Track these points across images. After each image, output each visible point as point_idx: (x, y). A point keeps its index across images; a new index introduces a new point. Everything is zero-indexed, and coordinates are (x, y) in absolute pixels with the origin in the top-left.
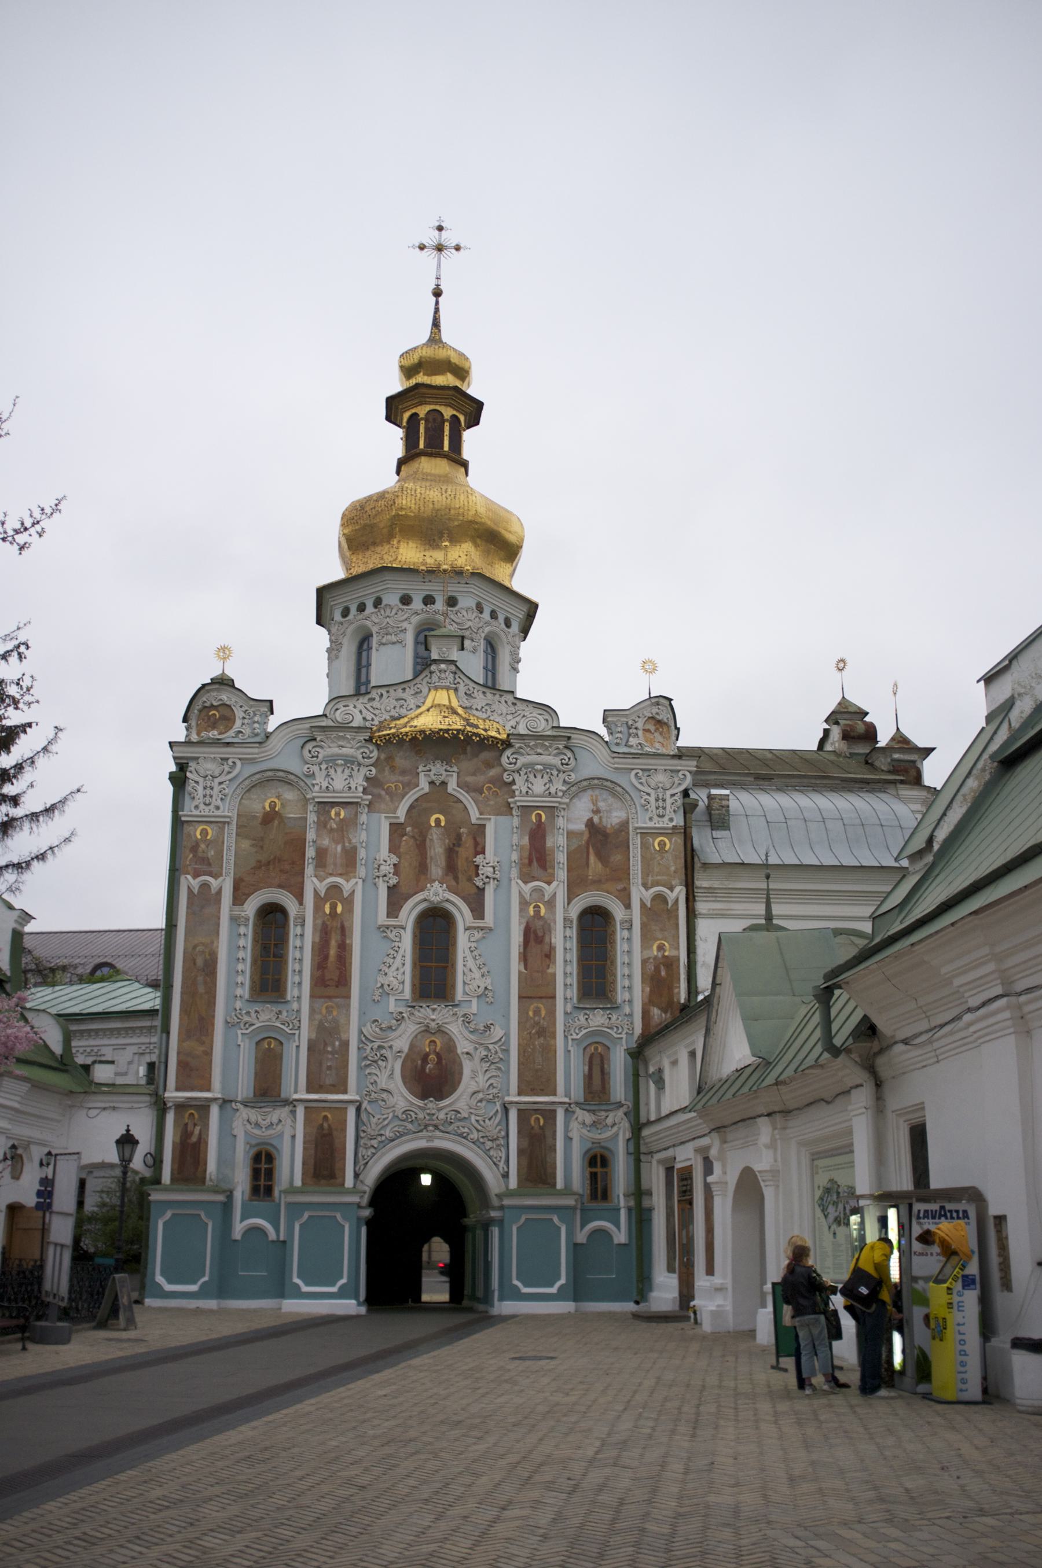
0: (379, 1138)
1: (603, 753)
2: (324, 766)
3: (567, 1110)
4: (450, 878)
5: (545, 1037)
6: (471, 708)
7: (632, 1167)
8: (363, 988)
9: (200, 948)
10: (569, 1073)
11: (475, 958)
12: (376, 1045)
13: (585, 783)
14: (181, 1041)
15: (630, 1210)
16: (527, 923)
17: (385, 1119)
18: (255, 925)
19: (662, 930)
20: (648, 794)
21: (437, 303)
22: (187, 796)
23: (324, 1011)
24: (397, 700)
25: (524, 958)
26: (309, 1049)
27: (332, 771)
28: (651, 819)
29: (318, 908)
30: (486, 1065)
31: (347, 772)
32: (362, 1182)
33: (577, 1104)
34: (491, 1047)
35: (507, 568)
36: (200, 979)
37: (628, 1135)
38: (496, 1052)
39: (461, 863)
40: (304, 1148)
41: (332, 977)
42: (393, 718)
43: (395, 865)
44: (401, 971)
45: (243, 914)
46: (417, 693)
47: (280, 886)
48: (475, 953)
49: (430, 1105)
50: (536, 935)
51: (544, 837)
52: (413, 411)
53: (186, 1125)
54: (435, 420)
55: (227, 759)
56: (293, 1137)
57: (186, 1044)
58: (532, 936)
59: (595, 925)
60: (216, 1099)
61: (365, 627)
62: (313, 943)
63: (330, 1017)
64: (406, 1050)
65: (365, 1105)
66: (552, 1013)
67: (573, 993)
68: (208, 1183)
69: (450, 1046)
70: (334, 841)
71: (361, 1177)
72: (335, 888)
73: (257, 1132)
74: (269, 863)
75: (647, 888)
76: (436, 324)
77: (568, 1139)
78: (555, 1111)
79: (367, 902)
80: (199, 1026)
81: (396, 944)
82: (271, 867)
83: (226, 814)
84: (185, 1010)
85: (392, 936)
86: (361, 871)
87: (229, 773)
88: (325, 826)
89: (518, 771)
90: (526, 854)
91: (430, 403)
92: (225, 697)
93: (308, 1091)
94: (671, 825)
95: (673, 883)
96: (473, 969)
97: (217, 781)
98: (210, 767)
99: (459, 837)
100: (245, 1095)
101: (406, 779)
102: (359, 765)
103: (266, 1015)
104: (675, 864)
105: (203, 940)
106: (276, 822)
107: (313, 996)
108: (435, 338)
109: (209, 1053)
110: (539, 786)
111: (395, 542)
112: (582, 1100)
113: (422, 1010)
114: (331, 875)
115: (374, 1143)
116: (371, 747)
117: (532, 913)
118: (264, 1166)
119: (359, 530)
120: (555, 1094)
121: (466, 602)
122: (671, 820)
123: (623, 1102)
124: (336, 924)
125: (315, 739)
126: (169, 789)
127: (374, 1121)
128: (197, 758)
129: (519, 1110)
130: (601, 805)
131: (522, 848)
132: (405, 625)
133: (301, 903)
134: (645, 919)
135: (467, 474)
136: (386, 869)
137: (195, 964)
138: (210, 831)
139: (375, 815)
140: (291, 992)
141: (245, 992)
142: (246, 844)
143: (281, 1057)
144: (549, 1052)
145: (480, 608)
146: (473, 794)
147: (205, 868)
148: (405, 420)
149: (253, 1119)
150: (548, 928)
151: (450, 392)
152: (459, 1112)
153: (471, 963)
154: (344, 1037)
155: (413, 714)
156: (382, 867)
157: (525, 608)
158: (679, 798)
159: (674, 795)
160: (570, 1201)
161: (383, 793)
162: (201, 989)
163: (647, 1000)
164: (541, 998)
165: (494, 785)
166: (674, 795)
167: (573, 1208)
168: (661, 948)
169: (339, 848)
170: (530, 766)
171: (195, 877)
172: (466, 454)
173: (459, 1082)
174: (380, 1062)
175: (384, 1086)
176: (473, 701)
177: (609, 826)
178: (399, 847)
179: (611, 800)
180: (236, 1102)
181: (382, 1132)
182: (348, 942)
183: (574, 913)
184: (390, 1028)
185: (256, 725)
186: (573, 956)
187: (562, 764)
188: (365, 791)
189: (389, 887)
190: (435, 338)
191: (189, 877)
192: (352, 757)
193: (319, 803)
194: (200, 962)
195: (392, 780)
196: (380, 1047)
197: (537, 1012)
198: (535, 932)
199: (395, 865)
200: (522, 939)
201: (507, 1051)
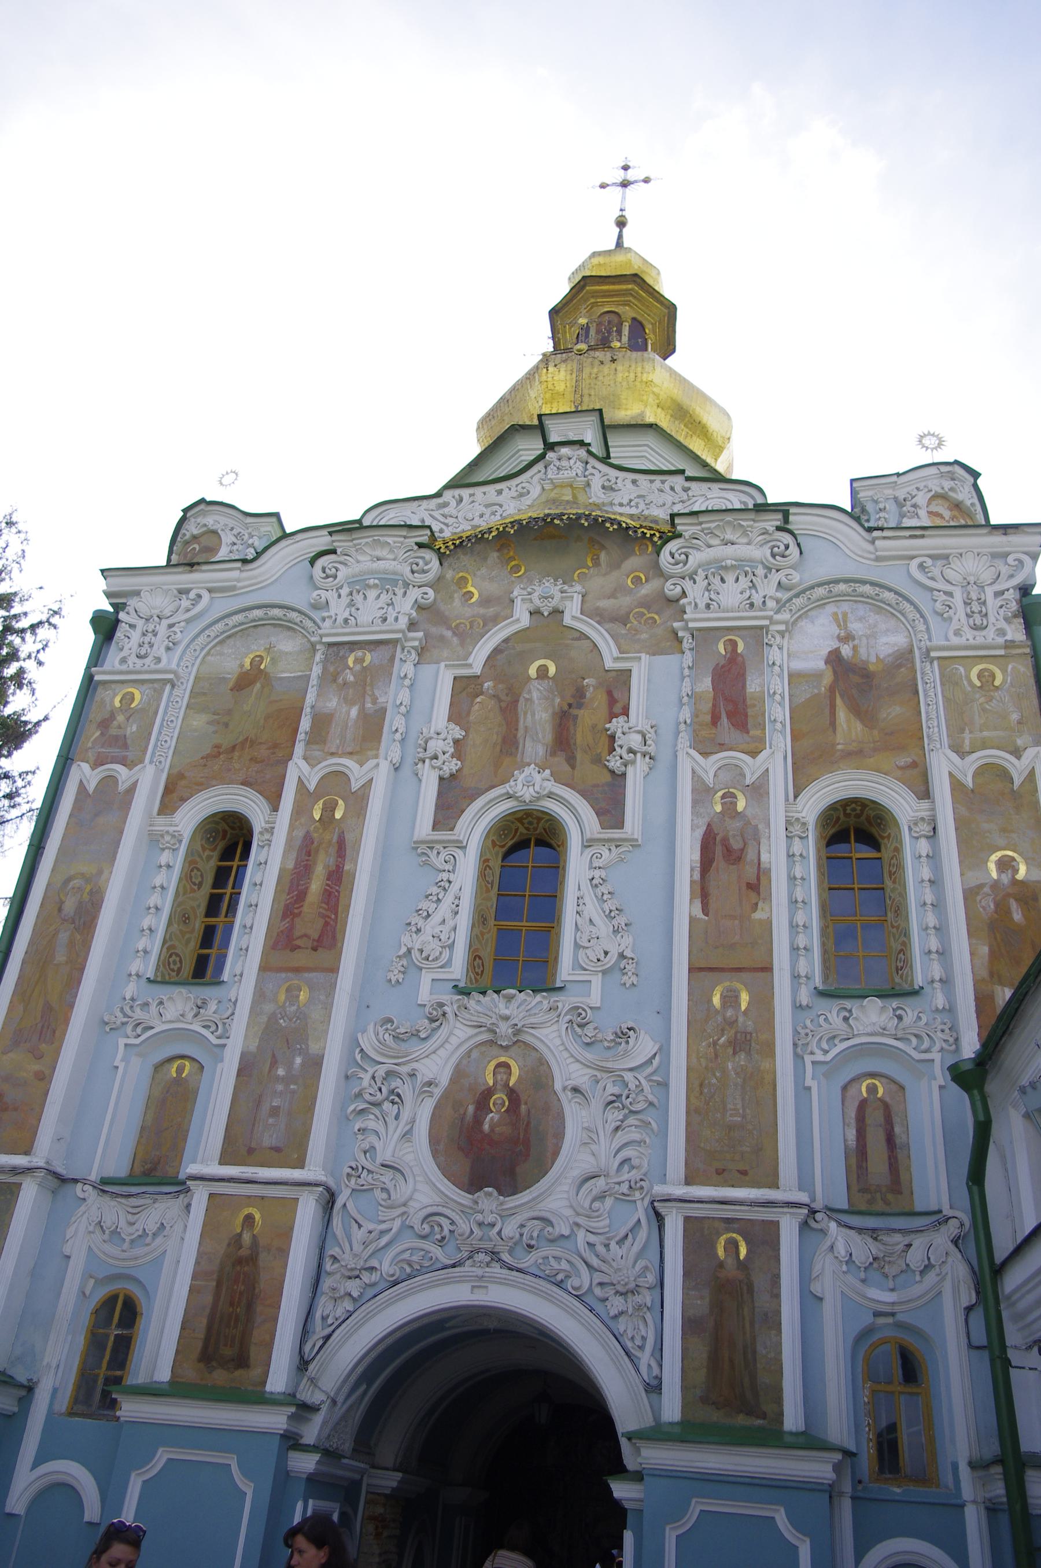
0: (366, 1278)
2: (344, 592)
3: (804, 1225)
4: (560, 760)
5: (749, 1053)
6: (611, 504)
9: (76, 883)
10: (808, 1145)
11: (602, 900)
13: (821, 591)
16: (709, 825)
17: (383, 1233)
18: (190, 852)
19: (1004, 830)
20: (950, 594)
21: (621, 232)
23: (282, 997)
24: (487, 506)
25: (703, 892)
26: (240, 1073)
27: (358, 598)
29: (300, 810)
30: (614, 1116)
32: (312, 1381)
33: (831, 1211)
34: (628, 1076)
36: (63, 937)
37: (967, 1296)
39: (581, 736)
40: (191, 1290)
41: (310, 932)
43: (456, 742)
44: (450, 924)
45: (171, 829)
46: (521, 495)
50: (728, 851)
51: (742, 677)
58: (719, 850)
59: (855, 832)
62: (282, 870)
63: (294, 1008)
64: (444, 1080)
66: (764, 1001)
67: (813, 965)
69: (540, 1076)
71: (311, 1367)
72: (340, 776)
74: (234, 747)
75: (962, 754)
77: (810, 1300)
78: (776, 1224)
81: (445, 876)
82: (236, 754)
83: (174, 666)
85: (438, 862)
86: (390, 750)
87: (188, 610)
88: (335, 681)
92: (211, 521)
93: (225, 1159)
94: (1000, 640)
95: (1019, 742)
96: (597, 920)
97: (165, 623)
100: (111, 1172)
106: (258, 685)
107: (264, 968)
109: (44, 1078)
110: (731, 593)
113: (485, 1000)
114: (332, 754)
115: (354, 1287)
117: (718, 808)
120: (774, 1185)
123: (947, 1211)
126: (88, 637)
127: (358, 1235)
128: (137, 593)
129: (687, 1219)
130: (855, 627)
137: (60, 910)
138: (138, 696)
139: (427, 670)
142: (199, 721)
144: (760, 1087)
146: (609, 626)
147: (115, 751)
149: (108, 1222)
150: (752, 834)
151: (630, 286)
152: (550, 1223)
153: (591, 908)
154: (314, 1048)
156: (431, 744)
158: (1012, 595)
159: (1002, 593)
160: (818, 1468)
162: (60, 957)
163: (984, 973)
164: (739, 970)
165: (648, 608)
166: (1002, 593)
167: (831, 1492)
168: (1005, 865)
169: (354, 712)
171: (96, 764)
173: (556, 1154)
174: (387, 1106)
176: (614, 494)
177: (873, 659)
178: (468, 714)
179: (873, 617)
180: (84, 1181)
181: (374, 1263)
182: (347, 867)
184: (415, 1034)
186: (811, 891)
187: (773, 556)
188: (412, 625)
189: (441, 779)
191: (85, 766)
192: (395, 573)
193: (330, 645)
194: (70, 906)
196: (389, 1074)
197: (731, 999)
199: (456, 742)
200: (697, 856)
201: (665, 1085)
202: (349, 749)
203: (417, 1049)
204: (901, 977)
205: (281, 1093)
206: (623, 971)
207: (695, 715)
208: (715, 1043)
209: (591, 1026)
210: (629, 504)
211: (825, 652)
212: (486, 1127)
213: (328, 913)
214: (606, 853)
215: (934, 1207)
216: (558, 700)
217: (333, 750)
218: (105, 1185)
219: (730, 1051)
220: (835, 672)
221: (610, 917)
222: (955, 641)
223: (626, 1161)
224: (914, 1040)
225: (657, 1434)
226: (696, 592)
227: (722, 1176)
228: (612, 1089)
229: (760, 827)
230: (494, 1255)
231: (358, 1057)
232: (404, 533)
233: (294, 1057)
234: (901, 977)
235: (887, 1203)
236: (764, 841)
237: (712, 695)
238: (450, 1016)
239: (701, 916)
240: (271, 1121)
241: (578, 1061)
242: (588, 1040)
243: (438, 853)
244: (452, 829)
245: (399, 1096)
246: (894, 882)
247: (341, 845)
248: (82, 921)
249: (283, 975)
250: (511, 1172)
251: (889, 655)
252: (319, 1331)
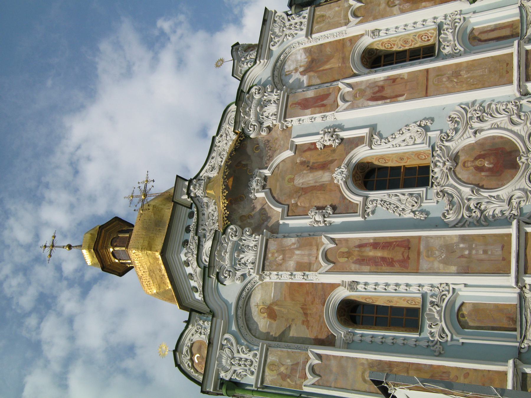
4: (332, 166)
5: (460, 71)
16: (368, 100)
19: (379, 5)
25: (394, 98)
27: (243, 261)
28: (302, 30)
30: (486, 117)
34: (469, 115)
38: (475, 110)
39: (321, 160)
46: (207, 206)
52: (111, 255)
55: (222, 345)
60: (515, 366)
63: (437, 252)
70: (290, 258)
74: (306, 314)
75: (349, 22)
82: (309, 312)
87: (232, 344)
88: (281, 265)
89: (261, 124)
90: (317, 109)
97: (236, 355)
99: (303, 163)
102: (241, 240)
105: (360, 373)
106: (276, 308)
107: (417, 272)
114: (316, 258)
116: (229, 230)
119: (153, 281)
122: (304, 17)
124: (356, 251)
133: (338, 285)
134: (370, 18)
147: (300, 368)
151: (103, 231)
158: (290, 18)
169: (297, 252)
171: (305, 378)
173: (502, 137)
174: (483, 207)
176: (216, 165)
177: (306, 60)
178: (305, 207)
182: (372, 241)
191: (305, 383)
193: (263, 270)
196: (469, 209)
198: (374, 93)
199: (317, 209)
202: (315, 251)
204: (431, 37)
205: (477, 251)
206: (425, 126)
208: (457, 83)
209: (448, 132)
210: (222, 158)
212: (491, 166)
213: (393, 246)
214: (374, 140)
215: (517, 11)
216: (305, 172)
217: (315, 258)
219: (460, 77)
220: (310, 72)
221: (403, 133)
223: (504, 110)
224: (457, 24)
227: (509, 71)
229: (370, 82)
231: (460, 224)
232: (216, 242)
233: (460, 248)
234: (431, 37)
235: (517, 28)
236: (376, 80)
237: (313, 109)
238: (442, 189)
239: (404, 97)
240: (489, 253)
241: (462, 135)
242: (454, 132)
243: (368, 208)
244: (357, 204)
245: (477, 204)
246: (394, 45)
247: (361, 246)
248: (387, 369)
249: (421, 261)
250: (510, 153)
251: (306, 55)
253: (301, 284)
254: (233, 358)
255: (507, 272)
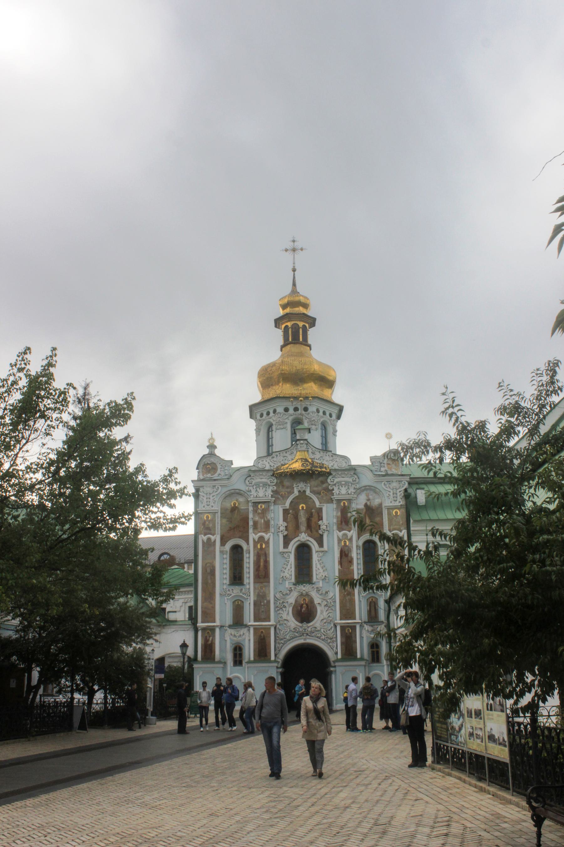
1: (369, 475)
2: (255, 487)
3: (361, 626)
7: (388, 648)
8: (275, 579)
11: (320, 564)
12: (281, 602)
14: (203, 603)
15: (388, 665)
18: (230, 554)
20: (390, 492)
21: (294, 274)
22: (200, 502)
25: (341, 563)
27: (258, 489)
28: (391, 502)
30: (326, 608)
31: (264, 489)
33: (365, 622)
35: (330, 391)
36: (209, 577)
39: (313, 524)
41: (262, 574)
42: (283, 465)
47: (240, 537)
48: (321, 562)
49: (304, 625)
53: (206, 637)
54: (296, 328)
56: (249, 640)
57: (205, 603)
58: (343, 554)
60: (217, 626)
61: (269, 422)
62: (254, 561)
64: (294, 603)
65: (278, 626)
68: (216, 660)
69: (312, 601)
72: (261, 538)
73: (234, 638)
74: (234, 528)
76: (294, 284)
77: (361, 638)
79: (275, 542)
80: (210, 596)
84: (204, 590)
86: (272, 530)
89: (335, 485)
90: (340, 519)
91: (293, 321)
92: (212, 460)
93: (255, 621)
94: (400, 504)
98: (209, 490)
99: (312, 514)
101: (289, 490)
102: (269, 485)
103: (236, 590)
104: (402, 520)
107: (255, 582)
108: (294, 291)
109: (214, 607)
110: (343, 490)
111: (281, 384)
112: (367, 620)
114: (260, 532)
115: (282, 641)
116: (274, 478)
118: (238, 652)
121: (312, 409)
122: (400, 502)
125: (250, 476)
127: (282, 632)
128: (203, 486)
130: (371, 497)
131: (338, 517)
132: (286, 421)
133: (248, 544)
135: (311, 349)
136: (282, 528)
138: (210, 516)
139: (276, 506)
140: (246, 581)
141: (227, 581)
142: (224, 521)
143: (243, 607)
144: (352, 602)
145: (318, 411)
147: (208, 531)
148: (283, 328)
149: (233, 633)
150: (350, 550)
153: (319, 566)
155: (290, 462)
157: (338, 408)
161: (279, 497)
169: (262, 521)
170: (340, 483)
171: (205, 535)
172: (310, 341)
173: (316, 615)
175: (285, 618)
179: (374, 494)
183: (361, 543)
184: (287, 594)
185: (226, 471)
188: (272, 496)
190: (294, 291)
193: (253, 502)
194: (208, 570)
195: (283, 491)
196: (283, 602)
201: (335, 602)
203: (288, 597)
207: (338, 521)
211: (364, 504)
218: (230, 626)
222: (391, 504)
225: (337, 660)
226: (336, 489)
228: (326, 603)
230: (307, 634)
252: (277, 649)
253: (248, 523)
254: (210, 494)
255: (255, 621)
